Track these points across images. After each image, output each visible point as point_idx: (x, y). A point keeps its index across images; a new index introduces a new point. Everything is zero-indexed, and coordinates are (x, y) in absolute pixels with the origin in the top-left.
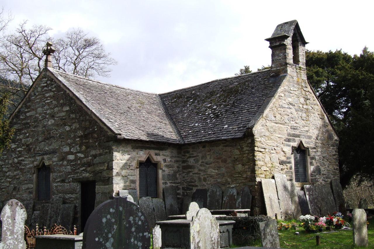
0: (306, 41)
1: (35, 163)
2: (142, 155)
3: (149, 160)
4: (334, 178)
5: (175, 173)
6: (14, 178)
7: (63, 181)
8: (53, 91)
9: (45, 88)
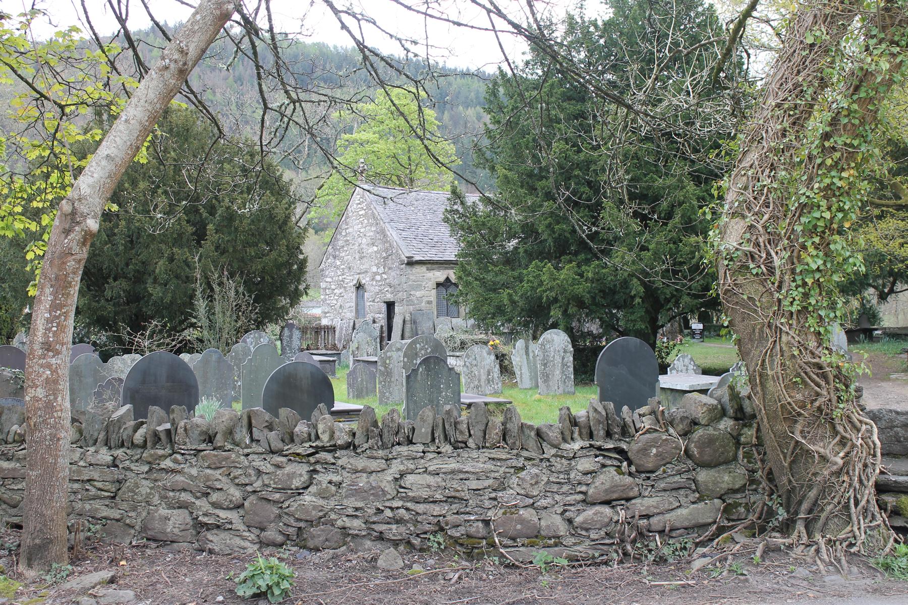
1: (355, 282)
3: (448, 279)
6: (341, 295)
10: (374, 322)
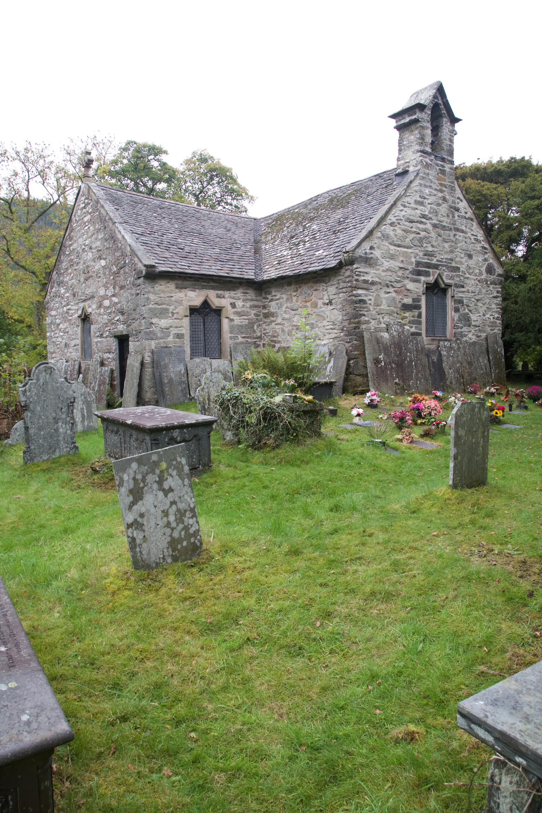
0: (457, 115)
1: (80, 312)
2: (194, 297)
3: (206, 304)
4: (492, 332)
5: (251, 324)
7: (101, 336)
8: (90, 213)
9: (84, 210)
10: (102, 364)
